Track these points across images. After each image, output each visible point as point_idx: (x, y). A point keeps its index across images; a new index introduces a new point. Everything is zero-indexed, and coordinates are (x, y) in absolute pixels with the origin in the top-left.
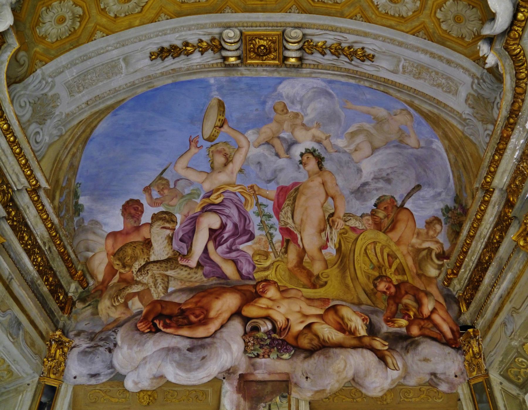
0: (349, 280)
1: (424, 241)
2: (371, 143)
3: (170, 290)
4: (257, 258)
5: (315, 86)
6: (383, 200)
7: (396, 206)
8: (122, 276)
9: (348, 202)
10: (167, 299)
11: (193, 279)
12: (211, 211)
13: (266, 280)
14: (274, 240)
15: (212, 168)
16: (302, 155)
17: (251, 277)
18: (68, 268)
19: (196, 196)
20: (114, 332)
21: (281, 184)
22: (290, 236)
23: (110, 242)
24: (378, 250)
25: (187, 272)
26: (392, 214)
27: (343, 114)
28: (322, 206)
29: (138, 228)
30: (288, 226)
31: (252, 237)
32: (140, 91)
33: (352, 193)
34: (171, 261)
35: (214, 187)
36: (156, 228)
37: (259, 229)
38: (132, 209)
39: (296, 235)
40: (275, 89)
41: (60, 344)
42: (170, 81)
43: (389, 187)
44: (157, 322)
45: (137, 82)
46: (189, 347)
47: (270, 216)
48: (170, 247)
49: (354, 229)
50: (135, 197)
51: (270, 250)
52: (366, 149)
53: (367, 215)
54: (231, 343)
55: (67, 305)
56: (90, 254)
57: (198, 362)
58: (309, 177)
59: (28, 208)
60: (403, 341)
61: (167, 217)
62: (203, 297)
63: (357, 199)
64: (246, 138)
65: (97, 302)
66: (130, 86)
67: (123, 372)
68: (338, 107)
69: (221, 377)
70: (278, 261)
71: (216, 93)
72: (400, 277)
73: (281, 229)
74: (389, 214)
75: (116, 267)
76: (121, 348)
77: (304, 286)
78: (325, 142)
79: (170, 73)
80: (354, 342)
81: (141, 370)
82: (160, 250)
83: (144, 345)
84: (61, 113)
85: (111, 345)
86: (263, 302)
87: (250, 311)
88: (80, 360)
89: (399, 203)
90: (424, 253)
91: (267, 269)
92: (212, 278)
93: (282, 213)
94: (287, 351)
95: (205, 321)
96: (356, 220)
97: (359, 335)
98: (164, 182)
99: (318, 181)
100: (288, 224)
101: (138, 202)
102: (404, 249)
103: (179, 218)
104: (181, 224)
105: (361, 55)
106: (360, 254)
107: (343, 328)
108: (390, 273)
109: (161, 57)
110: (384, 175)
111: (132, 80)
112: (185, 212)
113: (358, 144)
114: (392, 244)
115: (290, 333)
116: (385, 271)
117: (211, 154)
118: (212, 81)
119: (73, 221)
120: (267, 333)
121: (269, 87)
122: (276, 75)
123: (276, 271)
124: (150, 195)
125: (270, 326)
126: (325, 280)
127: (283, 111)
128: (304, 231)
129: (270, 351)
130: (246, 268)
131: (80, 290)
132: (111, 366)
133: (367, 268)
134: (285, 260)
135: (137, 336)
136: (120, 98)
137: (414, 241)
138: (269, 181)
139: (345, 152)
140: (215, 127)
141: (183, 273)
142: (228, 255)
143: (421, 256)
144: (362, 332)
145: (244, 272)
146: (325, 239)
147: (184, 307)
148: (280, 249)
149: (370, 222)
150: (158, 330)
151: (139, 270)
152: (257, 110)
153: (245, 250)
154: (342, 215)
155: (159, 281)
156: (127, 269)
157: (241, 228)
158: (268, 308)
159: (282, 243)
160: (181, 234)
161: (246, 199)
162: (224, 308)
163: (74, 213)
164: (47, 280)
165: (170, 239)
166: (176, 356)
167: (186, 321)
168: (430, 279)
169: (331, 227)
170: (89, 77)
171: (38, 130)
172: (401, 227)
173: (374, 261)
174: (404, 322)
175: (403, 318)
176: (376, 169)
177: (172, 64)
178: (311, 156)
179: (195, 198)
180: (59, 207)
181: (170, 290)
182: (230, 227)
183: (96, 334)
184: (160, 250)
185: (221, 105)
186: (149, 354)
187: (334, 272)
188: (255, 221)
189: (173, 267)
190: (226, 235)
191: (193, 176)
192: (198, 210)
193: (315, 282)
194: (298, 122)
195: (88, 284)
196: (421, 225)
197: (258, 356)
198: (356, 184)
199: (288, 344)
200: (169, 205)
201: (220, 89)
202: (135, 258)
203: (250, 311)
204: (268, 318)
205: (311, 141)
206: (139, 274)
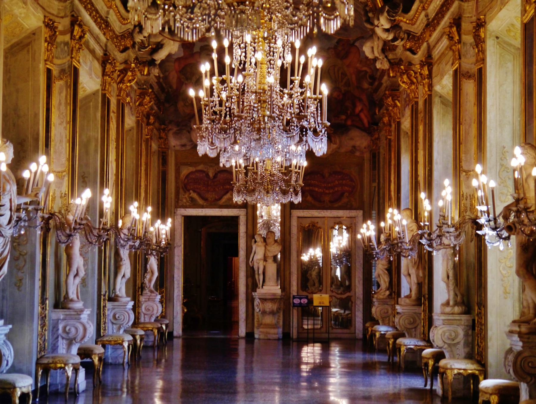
75: (183, 80)
89: (352, 42)
137: (358, 65)
149: (333, 53)
174: (344, 117)
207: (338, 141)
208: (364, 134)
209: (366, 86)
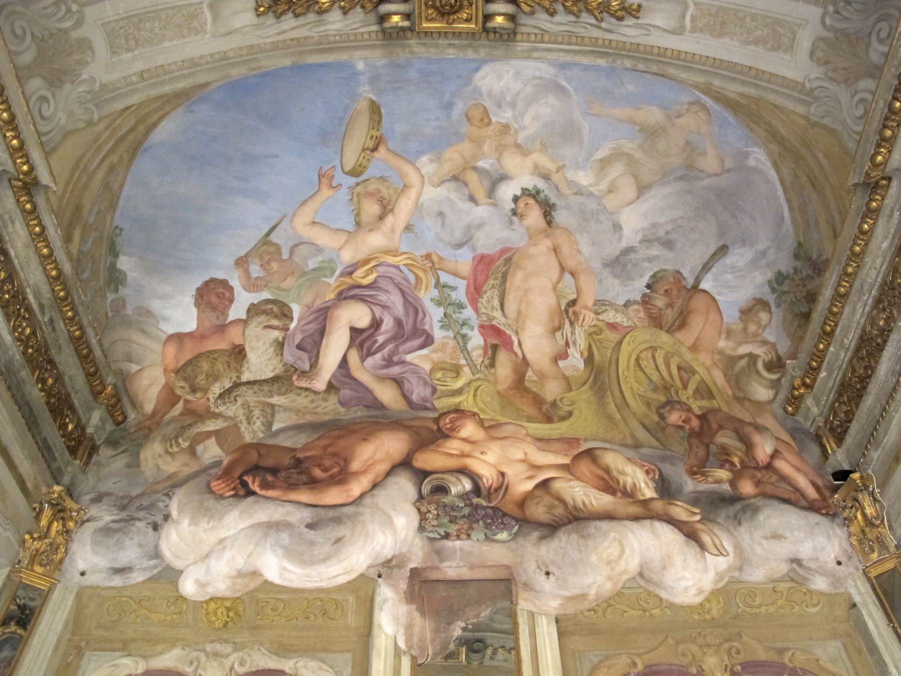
0: (612, 409)
1: (739, 344)
2: (636, 178)
3: (275, 427)
4: (439, 375)
5: (537, 74)
6: (661, 278)
7: (685, 287)
8: (189, 406)
9: (600, 281)
10: (270, 442)
11: (319, 410)
12: (353, 297)
13: (458, 411)
14: (470, 346)
15: (358, 224)
16: (516, 199)
17: (428, 405)
18: (88, 375)
19: (328, 273)
20: (167, 495)
21: (481, 251)
22: (498, 340)
23: (171, 350)
24: (660, 361)
25: (309, 399)
26: (680, 302)
27: (586, 126)
28: (555, 288)
29: (222, 328)
30: (494, 323)
31: (428, 341)
32: (236, 73)
33: (606, 265)
34: (280, 382)
35: (361, 256)
36: (254, 329)
37: (442, 327)
38: (213, 295)
39: (510, 337)
40: (468, 80)
41: (60, 511)
42: (287, 62)
43: (671, 255)
44: (249, 479)
45: (231, 54)
46: (309, 520)
47: (461, 306)
48: (279, 358)
49: (613, 326)
50: (220, 275)
51: (463, 362)
52: (628, 190)
53: (635, 302)
54: (393, 514)
55: (81, 446)
56: (134, 368)
57: (327, 548)
58: (530, 238)
59: (13, 222)
60: (724, 506)
61: (275, 309)
62: (339, 437)
63: (616, 276)
64: (418, 170)
65: (140, 446)
66: (220, 60)
67: (177, 564)
68: (577, 115)
69: (373, 573)
70: (478, 379)
71: (367, 88)
72: (705, 403)
73: (481, 327)
74: (673, 301)
75: (179, 392)
76: (177, 523)
77: (530, 419)
78: (555, 177)
79: (289, 47)
80: (633, 510)
81: (213, 561)
82: (261, 362)
83: (221, 519)
84: (93, 79)
85: (159, 519)
86: (453, 446)
87: (428, 460)
88: (96, 543)
89: (690, 282)
90: (743, 363)
91: (459, 392)
92: (356, 408)
93: (484, 300)
94: (504, 527)
95: (341, 477)
96: (617, 311)
97: (642, 498)
98: (272, 249)
99: (545, 244)
100: (494, 318)
101: (224, 283)
102: (705, 358)
103: (296, 310)
104: (299, 321)
105: (617, 7)
106: (628, 367)
107: (609, 484)
108: (686, 396)
109: (275, 12)
110: (661, 233)
111: (223, 49)
112: (308, 299)
113: (614, 180)
114: (684, 350)
115: (507, 497)
116: (677, 393)
117: (356, 199)
118: (360, 66)
119: (104, 297)
120: (464, 496)
121: (459, 77)
122: (470, 54)
123: (475, 395)
124: (247, 272)
125: (468, 485)
126: (568, 408)
127: (482, 120)
128: (523, 330)
129: (471, 528)
130: (418, 392)
131: (110, 427)
132: (157, 554)
133: (643, 389)
134: (491, 378)
135: (211, 502)
136: (201, 79)
137: (722, 344)
138: (459, 246)
139: (591, 194)
140: (364, 150)
141: (302, 401)
142: (385, 371)
143: (737, 368)
144: (649, 492)
145: (414, 398)
146: (563, 343)
147: (300, 455)
148: (480, 360)
149: (642, 315)
150: (250, 493)
151: (221, 396)
152: (437, 119)
153: (416, 362)
154: (590, 303)
155: (257, 412)
156: (199, 395)
157: (408, 327)
158: (463, 455)
159: (485, 349)
160: (298, 338)
161: (417, 278)
162: (378, 456)
163: (108, 284)
164: (43, 381)
165: (280, 345)
166: (285, 537)
167: (304, 478)
168: (758, 405)
169: (572, 323)
170: (148, 25)
171: (48, 94)
172: (697, 323)
173: (655, 377)
174: (724, 474)
175: (722, 467)
176: (646, 224)
177: (293, 28)
178: (531, 201)
179: (326, 276)
180: (79, 260)
181: (275, 427)
182: (388, 324)
183: (132, 499)
184: (261, 362)
185: (375, 110)
186: (232, 532)
187: (583, 398)
188: (436, 314)
189: (283, 390)
190: (381, 339)
191: (322, 238)
192: (332, 296)
193: (548, 412)
194: (509, 140)
195: (125, 418)
196: (731, 315)
197: (447, 536)
198: (613, 249)
199: (505, 514)
200: (279, 288)
201: (374, 80)
202: (215, 377)
203: (428, 460)
204: (463, 471)
205: (532, 174)
206: (219, 402)
207: (728, 545)
208: (814, 518)
209: (762, 393)
